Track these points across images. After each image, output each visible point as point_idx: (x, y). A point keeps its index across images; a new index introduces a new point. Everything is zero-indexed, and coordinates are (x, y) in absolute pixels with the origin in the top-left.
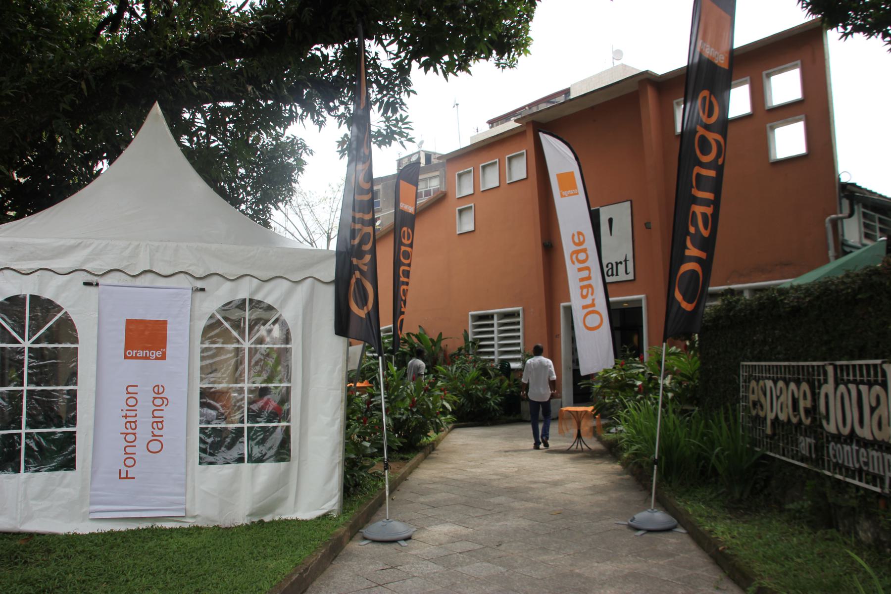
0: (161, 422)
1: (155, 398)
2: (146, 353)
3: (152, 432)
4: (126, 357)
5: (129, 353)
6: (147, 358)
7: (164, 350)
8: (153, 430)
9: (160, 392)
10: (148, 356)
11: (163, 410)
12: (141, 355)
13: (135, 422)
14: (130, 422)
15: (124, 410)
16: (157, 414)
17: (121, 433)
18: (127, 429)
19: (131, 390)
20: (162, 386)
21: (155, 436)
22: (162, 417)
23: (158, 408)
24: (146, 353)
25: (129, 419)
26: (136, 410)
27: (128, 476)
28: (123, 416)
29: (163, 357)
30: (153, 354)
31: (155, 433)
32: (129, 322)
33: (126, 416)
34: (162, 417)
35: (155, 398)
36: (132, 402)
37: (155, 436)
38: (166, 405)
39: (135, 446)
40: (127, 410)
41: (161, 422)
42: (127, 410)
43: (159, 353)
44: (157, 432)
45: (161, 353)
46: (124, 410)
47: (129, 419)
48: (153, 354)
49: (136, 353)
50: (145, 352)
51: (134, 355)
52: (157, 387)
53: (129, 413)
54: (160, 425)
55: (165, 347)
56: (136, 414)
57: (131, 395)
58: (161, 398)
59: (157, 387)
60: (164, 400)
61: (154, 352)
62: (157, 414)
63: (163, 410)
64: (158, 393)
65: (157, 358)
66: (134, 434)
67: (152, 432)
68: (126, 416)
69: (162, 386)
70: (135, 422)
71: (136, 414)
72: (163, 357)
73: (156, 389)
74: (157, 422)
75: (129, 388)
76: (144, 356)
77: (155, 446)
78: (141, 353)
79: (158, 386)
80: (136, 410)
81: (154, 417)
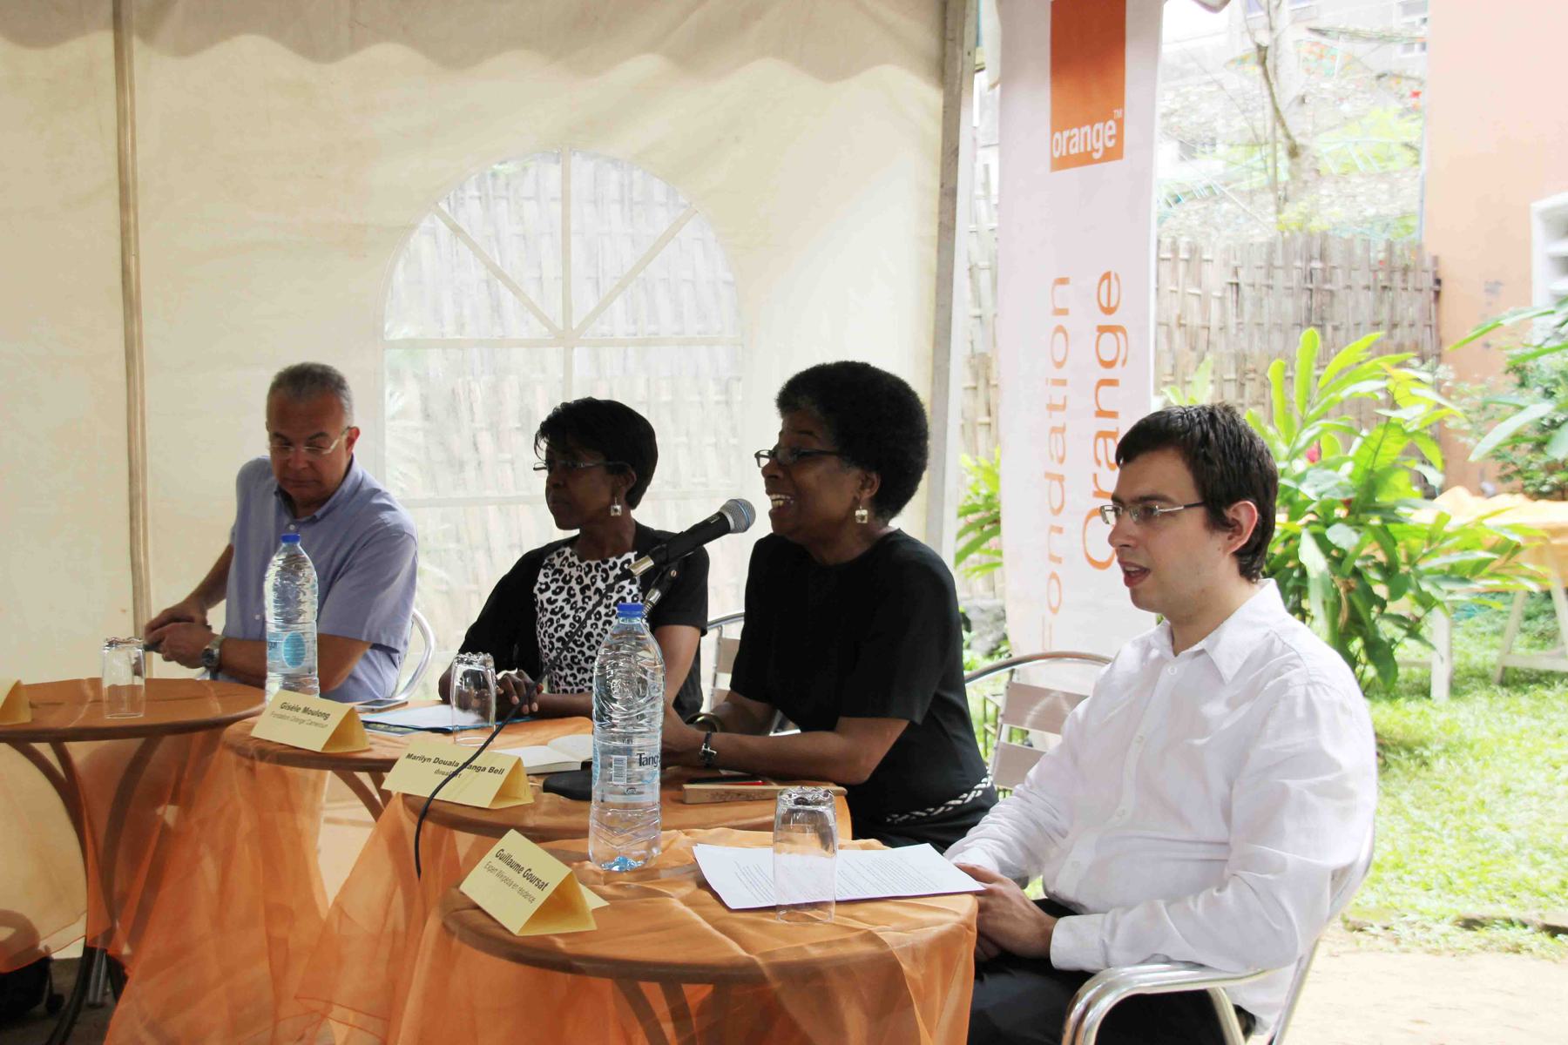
2: (1086, 134)
24: (1086, 134)
76: (1082, 150)
79: (1107, 276)
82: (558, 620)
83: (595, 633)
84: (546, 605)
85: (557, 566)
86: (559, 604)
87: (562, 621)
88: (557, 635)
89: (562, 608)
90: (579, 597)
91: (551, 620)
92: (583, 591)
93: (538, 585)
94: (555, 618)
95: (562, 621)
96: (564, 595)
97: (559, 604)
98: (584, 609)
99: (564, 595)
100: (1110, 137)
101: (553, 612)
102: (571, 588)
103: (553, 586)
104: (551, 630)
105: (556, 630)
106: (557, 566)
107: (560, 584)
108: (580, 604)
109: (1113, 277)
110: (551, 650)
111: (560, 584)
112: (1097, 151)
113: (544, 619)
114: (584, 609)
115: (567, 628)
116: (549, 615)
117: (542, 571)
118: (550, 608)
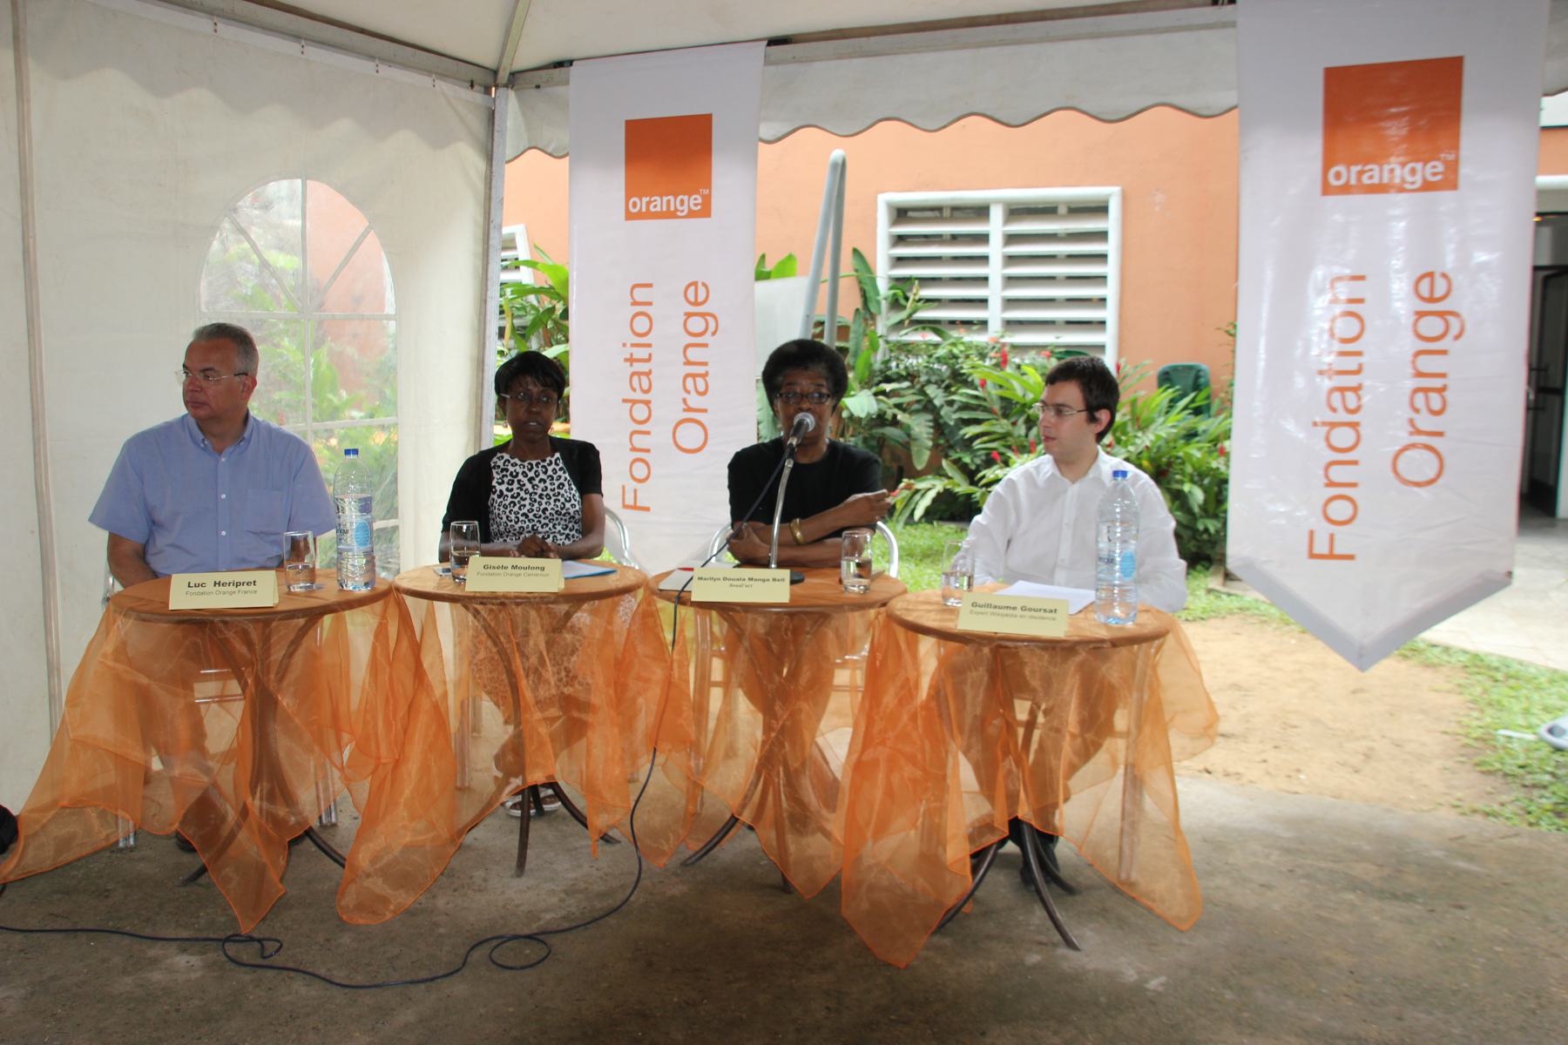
0: (704, 376)
1: (689, 315)
2: (669, 201)
3: (685, 401)
4: (630, 216)
5: (635, 205)
6: (670, 215)
7: (706, 192)
8: (686, 395)
9: (700, 299)
10: (672, 209)
11: (705, 345)
12: (658, 209)
13: (648, 374)
14: (639, 374)
15: (628, 345)
16: (693, 354)
17: (625, 401)
18: (634, 390)
19: (640, 295)
20: (704, 284)
21: (689, 409)
22: (705, 364)
23: (696, 340)
24: (669, 201)
25: (639, 367)
26: (649, 345)
27: (638, 504)
28: (626, 360)
29: (705, 211)
30: (682, 202)
31: (692, 404)
32: (629, 123)
33: (631, 360)
34: (705, 364)
35: (689, 315)
36: (641, 324)
37: (689, 409)
38: (714, 333)
39: (648, 433)
40: (633, 345)
41: (704, 376)
42: (633, 345)
43: (695, 201)
44: (694, 401)
45: (700, 201)
46: (628, 345)
47: (639, 367)
48: (682, 202)
49: (649, 203)
50: (665, 199)
51: (644, 210)
52: (692, 289)
53: (641, 353)
54: (700, 381)
55: (708, 185)
56: (650, 355)
57: (641, 308)
58: (703, 315)
59: (692, 289)
60: (708, 318)
61: (686, 198)
62: (693, 354)
63: (705, 345)
64: (696, 303)
65: (692, 214)
66: (647, 403)
67: (685, 401)
68: (631, 360)
69: (704, 284)
70: (648, 374)
71: (650, 355)
72: (705, 211)
73: (691, 297)
74: (694, 376)
75: (637, 290)
76: (665, 209)
77: (690, 435)
78: (659, 203)
79: (695, 284)
80: (649, 345)
81: (688, 363)
82: (519, 502)
83: (549, 508)
84: (505, 493)
85: (502, 466)
86: (515, 491)
87: (523, 503)
88: (521, 512)
89: (519, 494)
90: (529, 486)
91: (512, 502)
92: (531, 480)
93: (495, 480)
94: (516, 501)
95: (523, 503)
96: (516, 485)
97: (515, 491)
98: (536, 494)
99: (516, 485)
100: (696, 205)
101: (512, 497)
102: (519, 481)
103: (506, 480)
104: (516, 509)
105: (520, 509)
106: (502, 466)
107: (510, 478)
108: (531, 490)
109: (700, 285)
110: (516, 523)
111: (510, 478)
112: (682, 211)
113: (507, 503)
114: (536, 494)
115: (528, 507)
116: (510, 500)
117: (494, 471)
118: (510, 494)
